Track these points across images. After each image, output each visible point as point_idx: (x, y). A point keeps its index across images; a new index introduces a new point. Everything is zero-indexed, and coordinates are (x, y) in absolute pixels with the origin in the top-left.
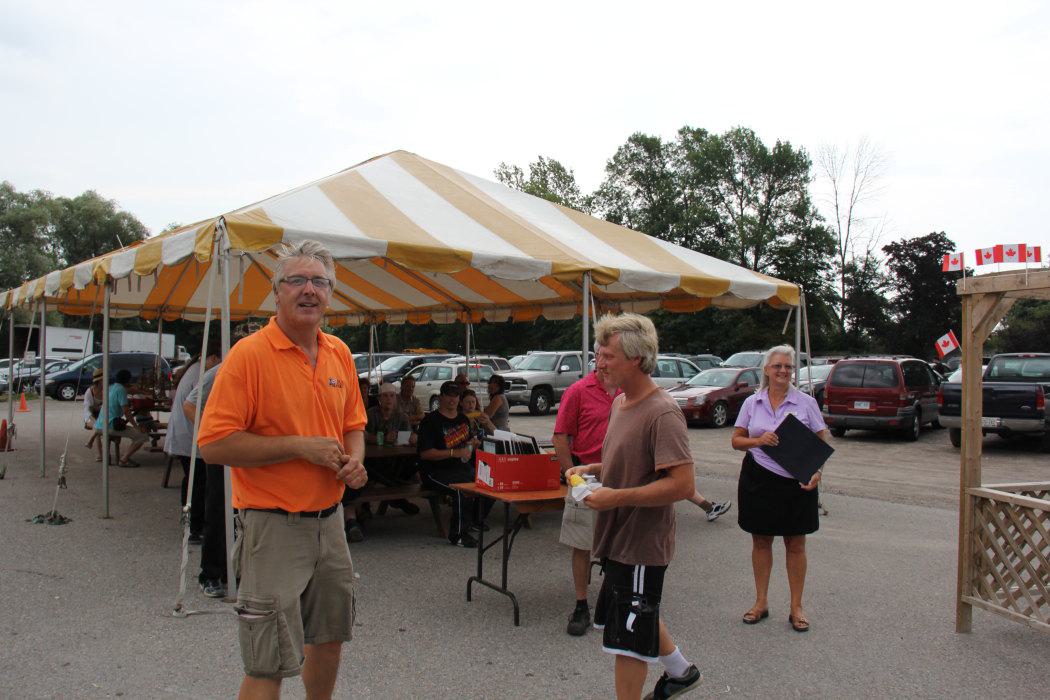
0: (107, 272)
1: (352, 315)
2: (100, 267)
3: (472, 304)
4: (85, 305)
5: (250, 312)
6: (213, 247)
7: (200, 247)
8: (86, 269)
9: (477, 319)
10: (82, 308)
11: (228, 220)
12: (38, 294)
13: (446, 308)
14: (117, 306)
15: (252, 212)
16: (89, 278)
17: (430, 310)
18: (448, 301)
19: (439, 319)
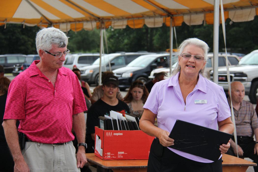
1: (87, 21)
3: (174, 10)
5: (6, 20)
9: (179, 23)
13: (154, 15)
17: (142, 16)
18: (154, 8)
19: (150, 23)
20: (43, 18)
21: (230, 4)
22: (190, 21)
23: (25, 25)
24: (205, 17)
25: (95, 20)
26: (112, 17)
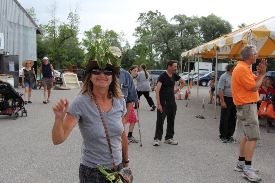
0: (217, 46)
2: (215, 44)
6: (247, 39)
7: (244, 38)
8: (211, 44)
11: (252, 30)
12: (197, 52)
14: (220, 55)
15: (261, 27)
16: (212, 48)
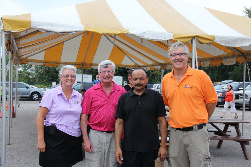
1: (156, 65)
4: (54, 63)
10: (53, 64)
20: (136, 65)
21: (223, 55)
22: (203, 64)
23: (127, 68)
24: (211, 63)
25: (159, 65)
26: (166, 63)
